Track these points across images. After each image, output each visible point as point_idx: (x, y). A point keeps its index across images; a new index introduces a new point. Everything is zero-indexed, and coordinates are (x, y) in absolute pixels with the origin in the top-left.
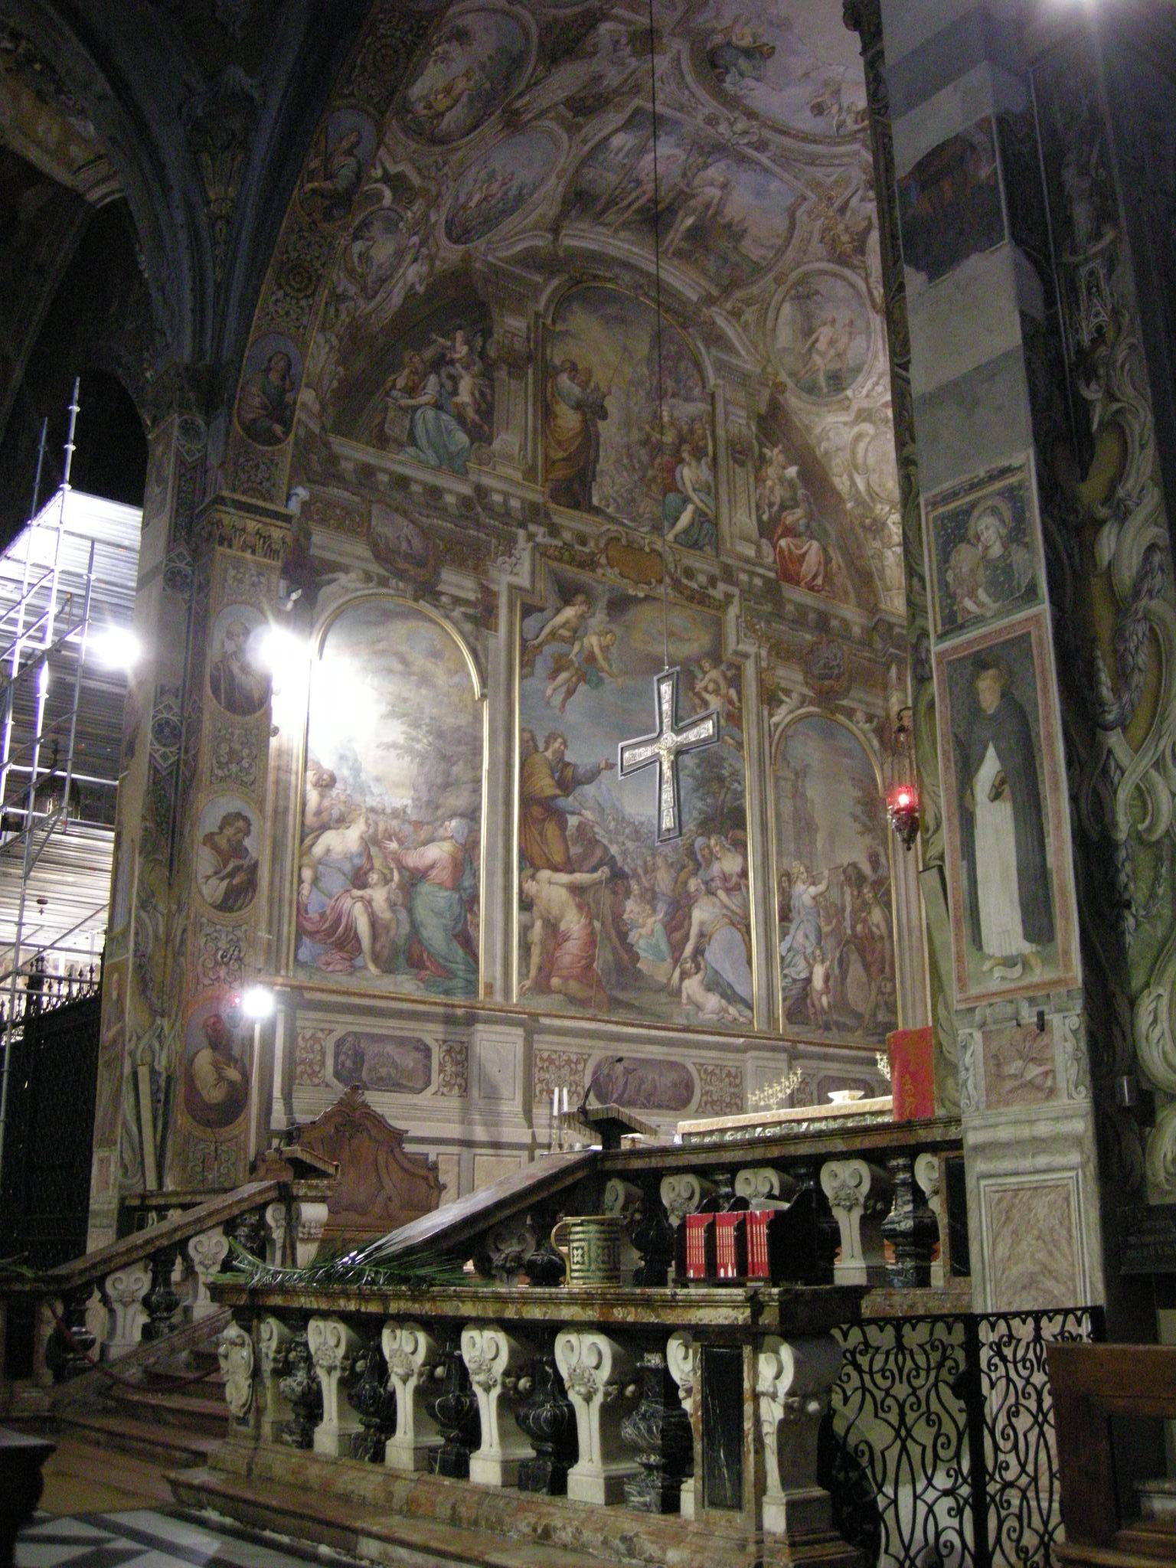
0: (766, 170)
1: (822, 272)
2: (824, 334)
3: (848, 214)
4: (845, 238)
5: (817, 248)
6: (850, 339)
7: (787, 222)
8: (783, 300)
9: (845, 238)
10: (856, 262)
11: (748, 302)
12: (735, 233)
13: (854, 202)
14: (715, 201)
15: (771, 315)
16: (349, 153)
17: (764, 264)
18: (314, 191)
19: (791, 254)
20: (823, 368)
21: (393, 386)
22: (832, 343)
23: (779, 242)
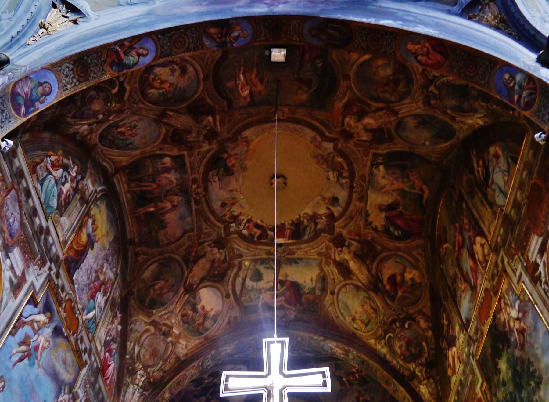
0: (191, 212)
1: (176, 260)
2: (161, 283)
3: (200, 247)
4: (193, 254)
5: (182, 251)
6: (169, 291)
7: (180, 235)
8: (156, 261)
9: (193, 254)
10: (190, 265)
11: (144, 253)
12: (162, 225)
13: (206, 244)
14: (167, 209)
15: (149, 263)
16: (139, 55)
17: (161, 243)
18: (117, 51)
19: (173, 246)
20: (151, 295)
21: (50, 156)
22: (161, 288)
23: (172, 240)
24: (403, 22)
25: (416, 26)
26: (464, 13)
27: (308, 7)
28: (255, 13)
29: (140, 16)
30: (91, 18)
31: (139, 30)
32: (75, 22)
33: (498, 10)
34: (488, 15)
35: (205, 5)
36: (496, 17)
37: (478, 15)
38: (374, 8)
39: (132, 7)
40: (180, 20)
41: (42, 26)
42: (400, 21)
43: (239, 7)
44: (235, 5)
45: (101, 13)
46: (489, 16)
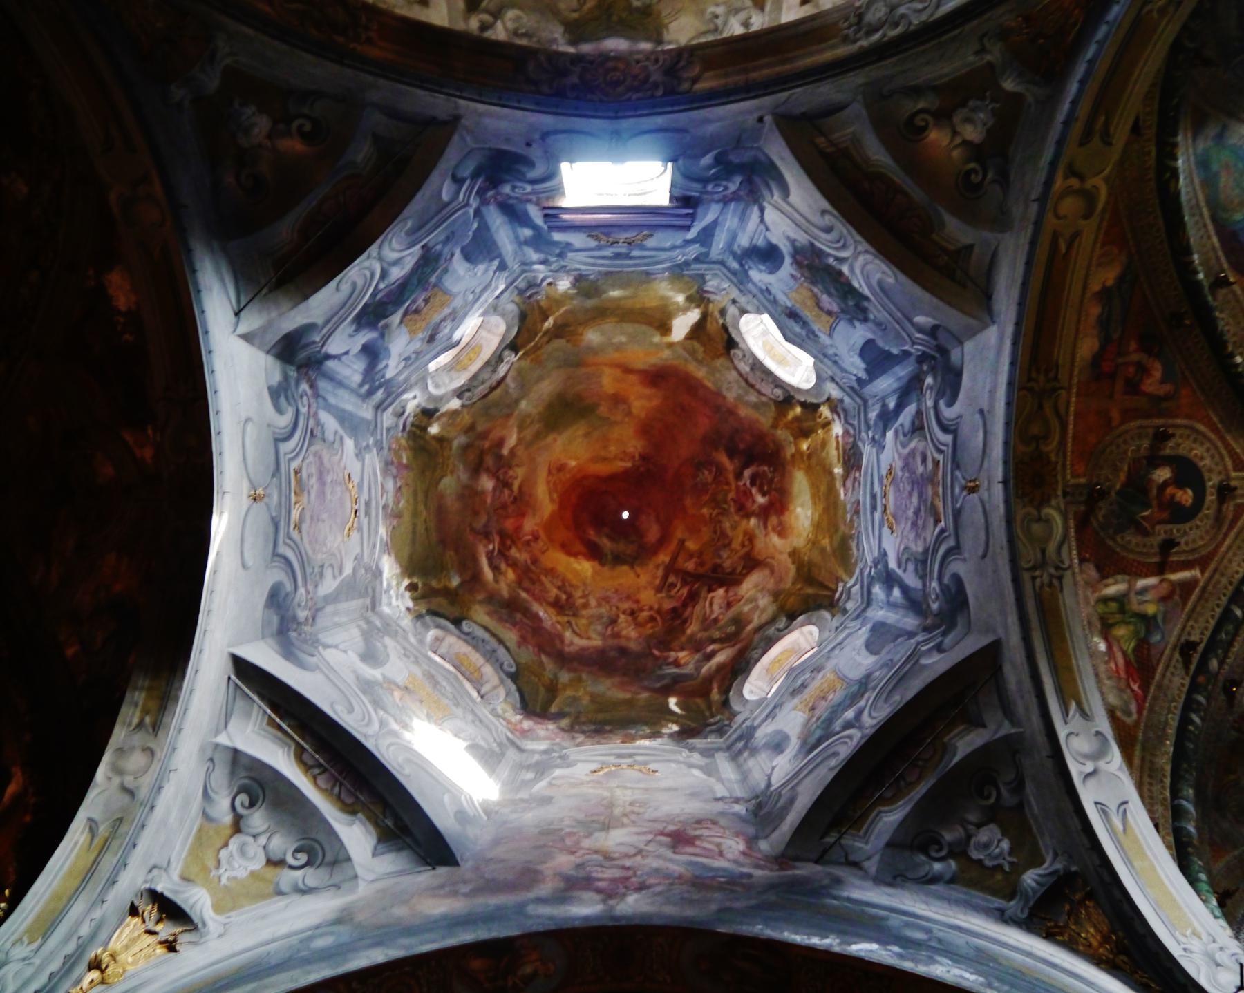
24: (901, 947)
25: (931, 961)
26: (1035, 920)
27: (691, 902)
28: (574, 919)
29: (318, 927)
30: (208, 933)
31: (309, 973)
32: (171, 946)
33: (1106, 921)
34: (1088, 932)
35: (466, 895)
36: (1106, 939)
37: (1066, 926)
38: (835, 902)
39: (306, 897)
40: (405, 941)
41: (95, 965)
42: (895, 944)
43: (540, 901)
44: (531, 895)
45: (235, 917)
46: (1090, 933)
